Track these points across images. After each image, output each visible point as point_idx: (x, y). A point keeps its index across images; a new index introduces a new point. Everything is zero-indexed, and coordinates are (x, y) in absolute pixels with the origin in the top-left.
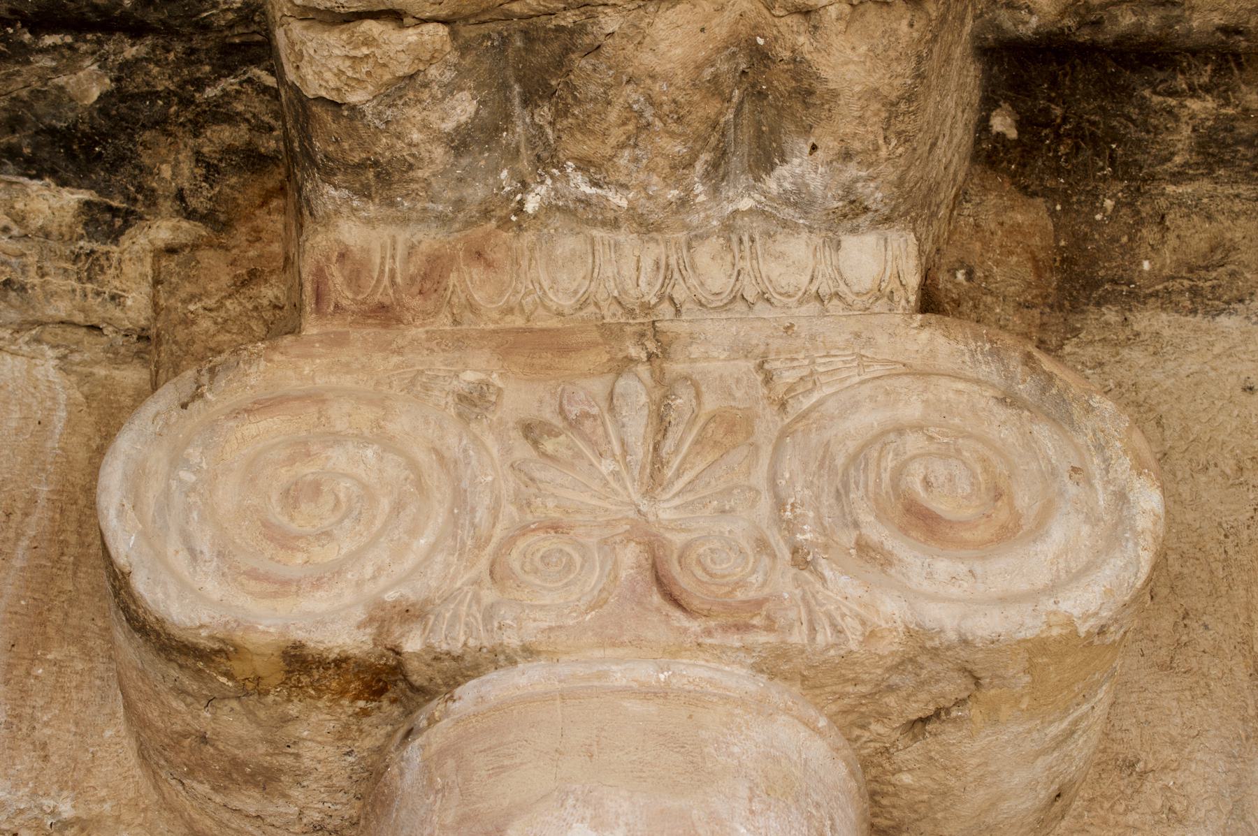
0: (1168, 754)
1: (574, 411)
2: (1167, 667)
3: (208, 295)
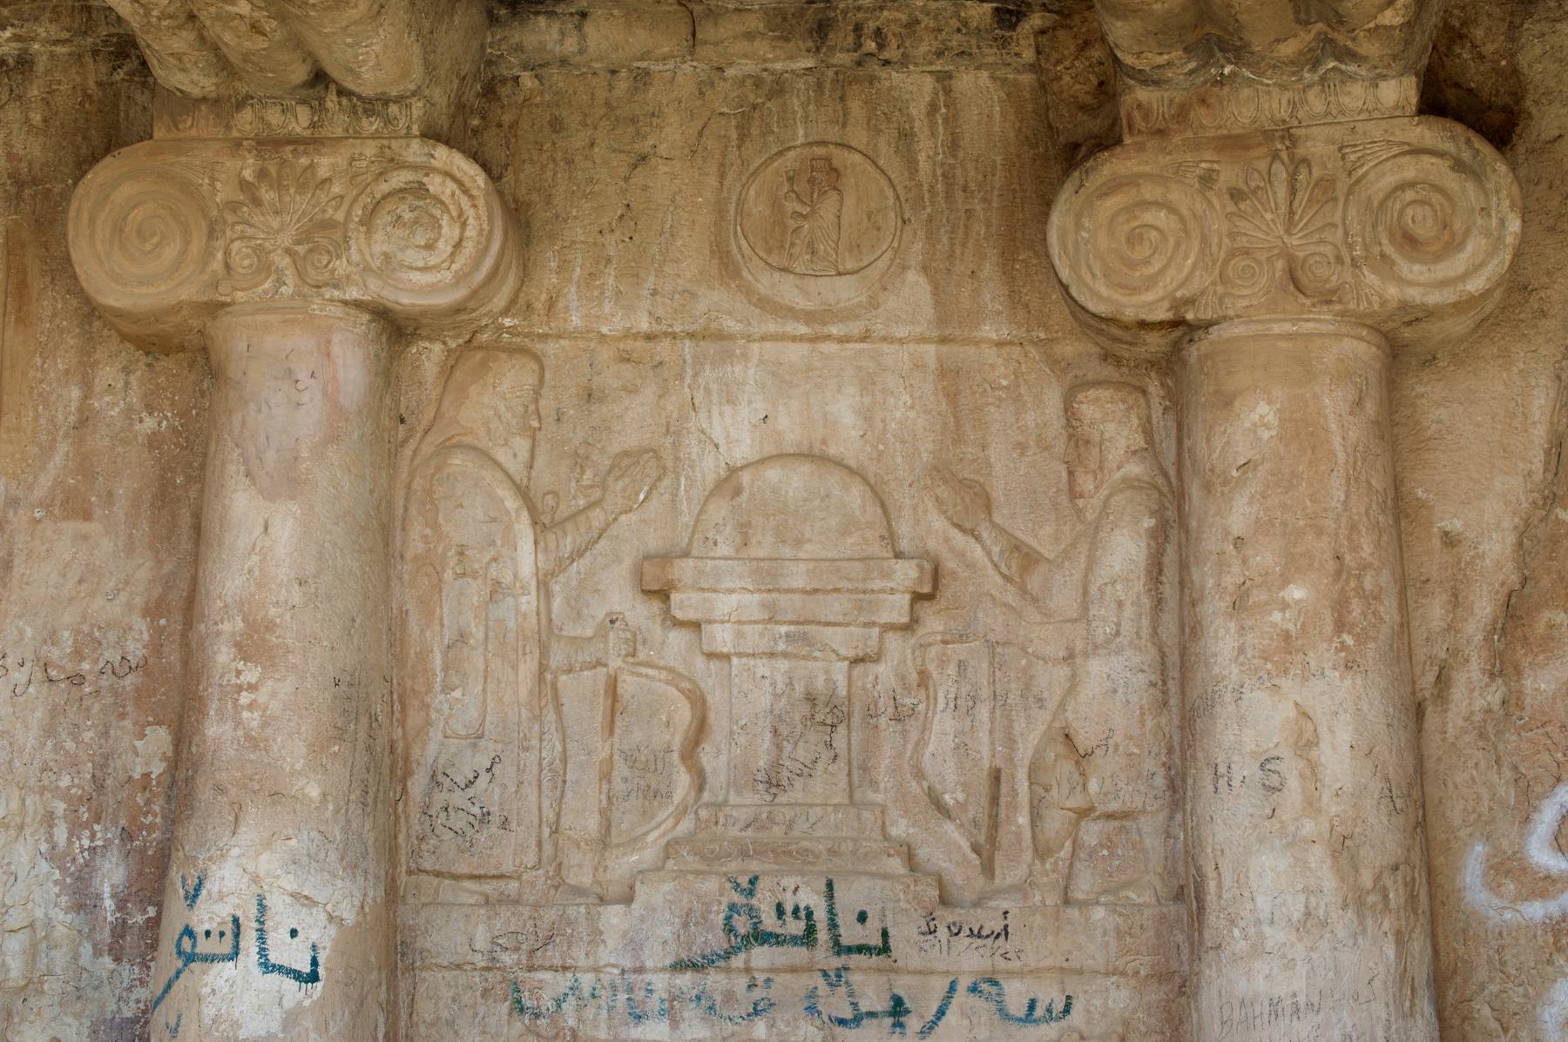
0: (1545, 279)
1: (1253, 185)
2: (1551, 229)
3: (1064, 58)
